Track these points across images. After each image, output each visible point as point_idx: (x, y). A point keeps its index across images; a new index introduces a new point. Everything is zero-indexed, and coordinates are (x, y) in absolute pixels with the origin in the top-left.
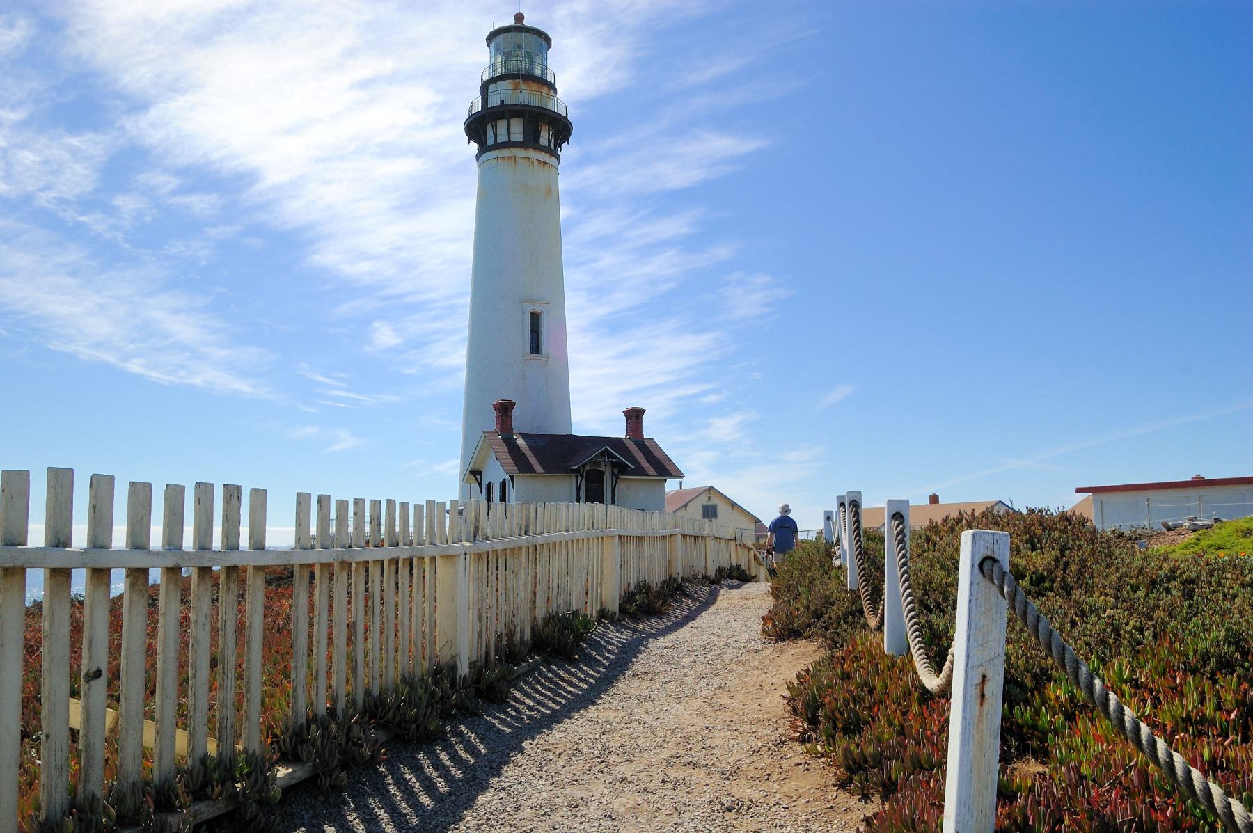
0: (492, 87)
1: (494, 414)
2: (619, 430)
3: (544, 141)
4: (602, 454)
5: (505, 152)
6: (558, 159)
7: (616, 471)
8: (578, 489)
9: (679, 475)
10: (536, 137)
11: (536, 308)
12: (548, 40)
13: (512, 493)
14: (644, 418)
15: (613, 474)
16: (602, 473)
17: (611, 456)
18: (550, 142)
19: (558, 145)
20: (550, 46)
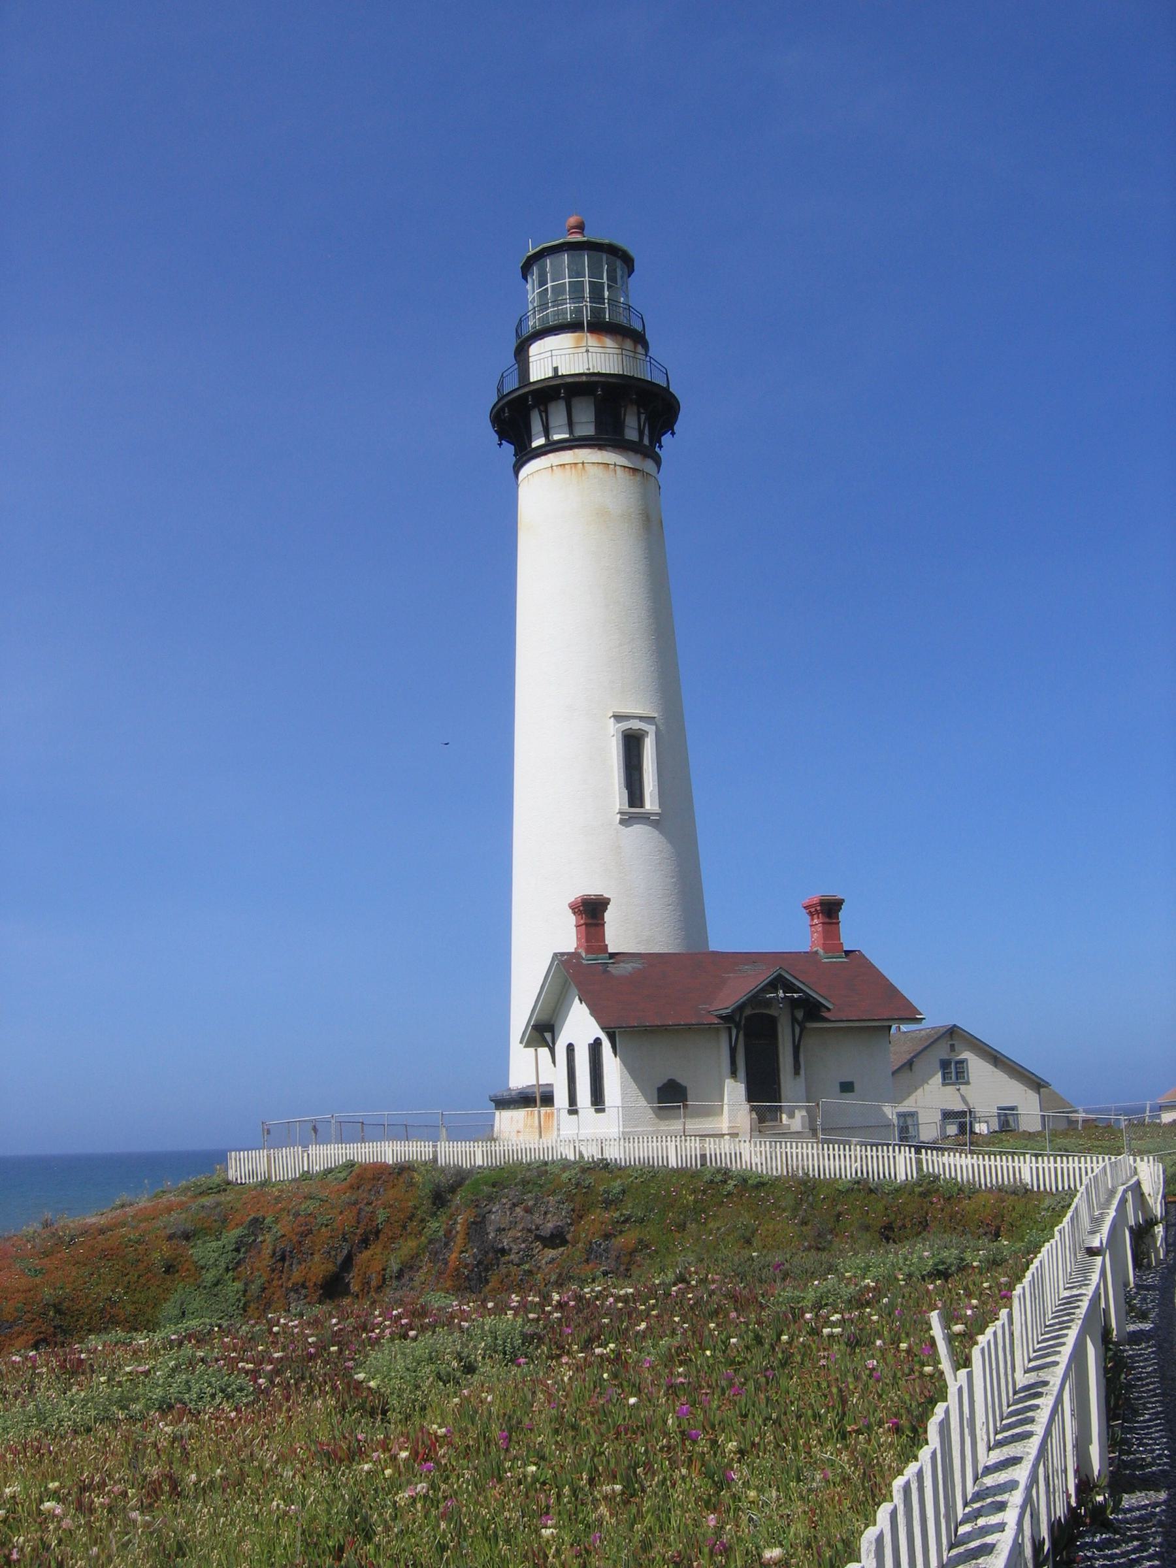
0: (535, 349)
1: (571, 919)
2: (798, 936)
3: (631, 434)
4: (773, 985)
5: (567, 456)
6: (658, 461)
7: (800, 1015)
8: (733, 1051)
9: (912, 1016)
10: (619, 427)
11: (636, 725)
12: (628, 261)
13: (612, 1064)
14: (842, 915)
15: (794, 1020)
16: (772, 1022)
17: (789, 987)
18: (641, 434)
19: (656, 439)
20: (631, 271)
